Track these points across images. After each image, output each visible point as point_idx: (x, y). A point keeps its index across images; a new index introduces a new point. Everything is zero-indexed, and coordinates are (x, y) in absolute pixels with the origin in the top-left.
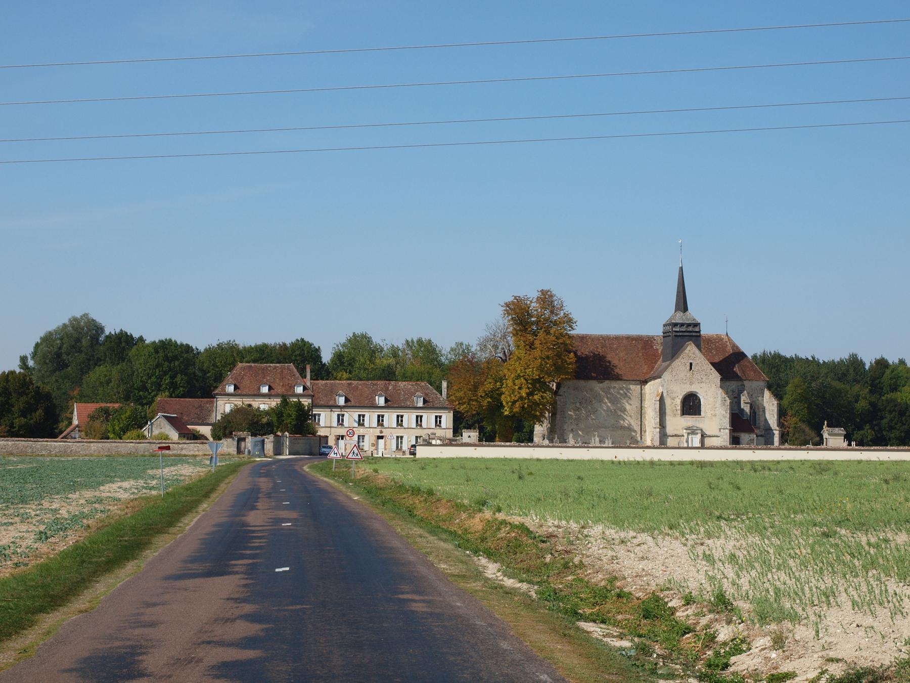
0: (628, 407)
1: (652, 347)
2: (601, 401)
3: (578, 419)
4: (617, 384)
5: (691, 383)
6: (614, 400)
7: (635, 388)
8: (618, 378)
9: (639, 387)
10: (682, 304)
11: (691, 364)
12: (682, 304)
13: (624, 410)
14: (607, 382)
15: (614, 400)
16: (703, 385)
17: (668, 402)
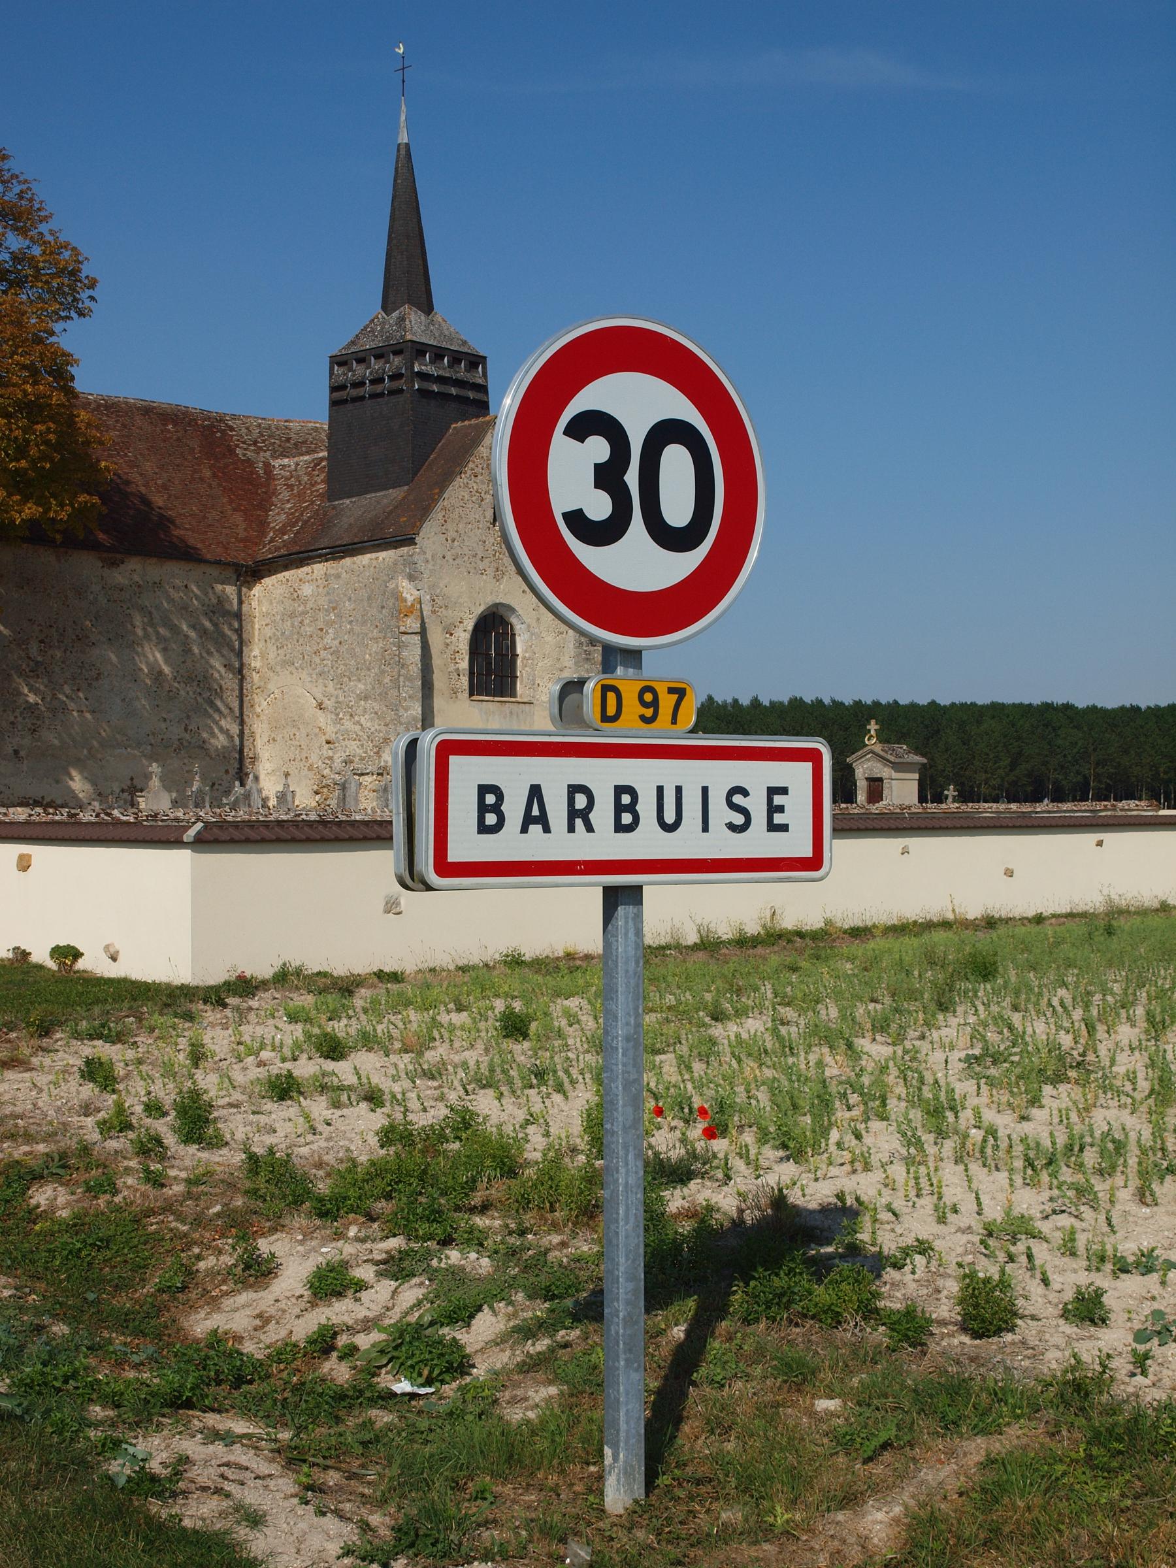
1: (231, 451)
17: (436, 638)
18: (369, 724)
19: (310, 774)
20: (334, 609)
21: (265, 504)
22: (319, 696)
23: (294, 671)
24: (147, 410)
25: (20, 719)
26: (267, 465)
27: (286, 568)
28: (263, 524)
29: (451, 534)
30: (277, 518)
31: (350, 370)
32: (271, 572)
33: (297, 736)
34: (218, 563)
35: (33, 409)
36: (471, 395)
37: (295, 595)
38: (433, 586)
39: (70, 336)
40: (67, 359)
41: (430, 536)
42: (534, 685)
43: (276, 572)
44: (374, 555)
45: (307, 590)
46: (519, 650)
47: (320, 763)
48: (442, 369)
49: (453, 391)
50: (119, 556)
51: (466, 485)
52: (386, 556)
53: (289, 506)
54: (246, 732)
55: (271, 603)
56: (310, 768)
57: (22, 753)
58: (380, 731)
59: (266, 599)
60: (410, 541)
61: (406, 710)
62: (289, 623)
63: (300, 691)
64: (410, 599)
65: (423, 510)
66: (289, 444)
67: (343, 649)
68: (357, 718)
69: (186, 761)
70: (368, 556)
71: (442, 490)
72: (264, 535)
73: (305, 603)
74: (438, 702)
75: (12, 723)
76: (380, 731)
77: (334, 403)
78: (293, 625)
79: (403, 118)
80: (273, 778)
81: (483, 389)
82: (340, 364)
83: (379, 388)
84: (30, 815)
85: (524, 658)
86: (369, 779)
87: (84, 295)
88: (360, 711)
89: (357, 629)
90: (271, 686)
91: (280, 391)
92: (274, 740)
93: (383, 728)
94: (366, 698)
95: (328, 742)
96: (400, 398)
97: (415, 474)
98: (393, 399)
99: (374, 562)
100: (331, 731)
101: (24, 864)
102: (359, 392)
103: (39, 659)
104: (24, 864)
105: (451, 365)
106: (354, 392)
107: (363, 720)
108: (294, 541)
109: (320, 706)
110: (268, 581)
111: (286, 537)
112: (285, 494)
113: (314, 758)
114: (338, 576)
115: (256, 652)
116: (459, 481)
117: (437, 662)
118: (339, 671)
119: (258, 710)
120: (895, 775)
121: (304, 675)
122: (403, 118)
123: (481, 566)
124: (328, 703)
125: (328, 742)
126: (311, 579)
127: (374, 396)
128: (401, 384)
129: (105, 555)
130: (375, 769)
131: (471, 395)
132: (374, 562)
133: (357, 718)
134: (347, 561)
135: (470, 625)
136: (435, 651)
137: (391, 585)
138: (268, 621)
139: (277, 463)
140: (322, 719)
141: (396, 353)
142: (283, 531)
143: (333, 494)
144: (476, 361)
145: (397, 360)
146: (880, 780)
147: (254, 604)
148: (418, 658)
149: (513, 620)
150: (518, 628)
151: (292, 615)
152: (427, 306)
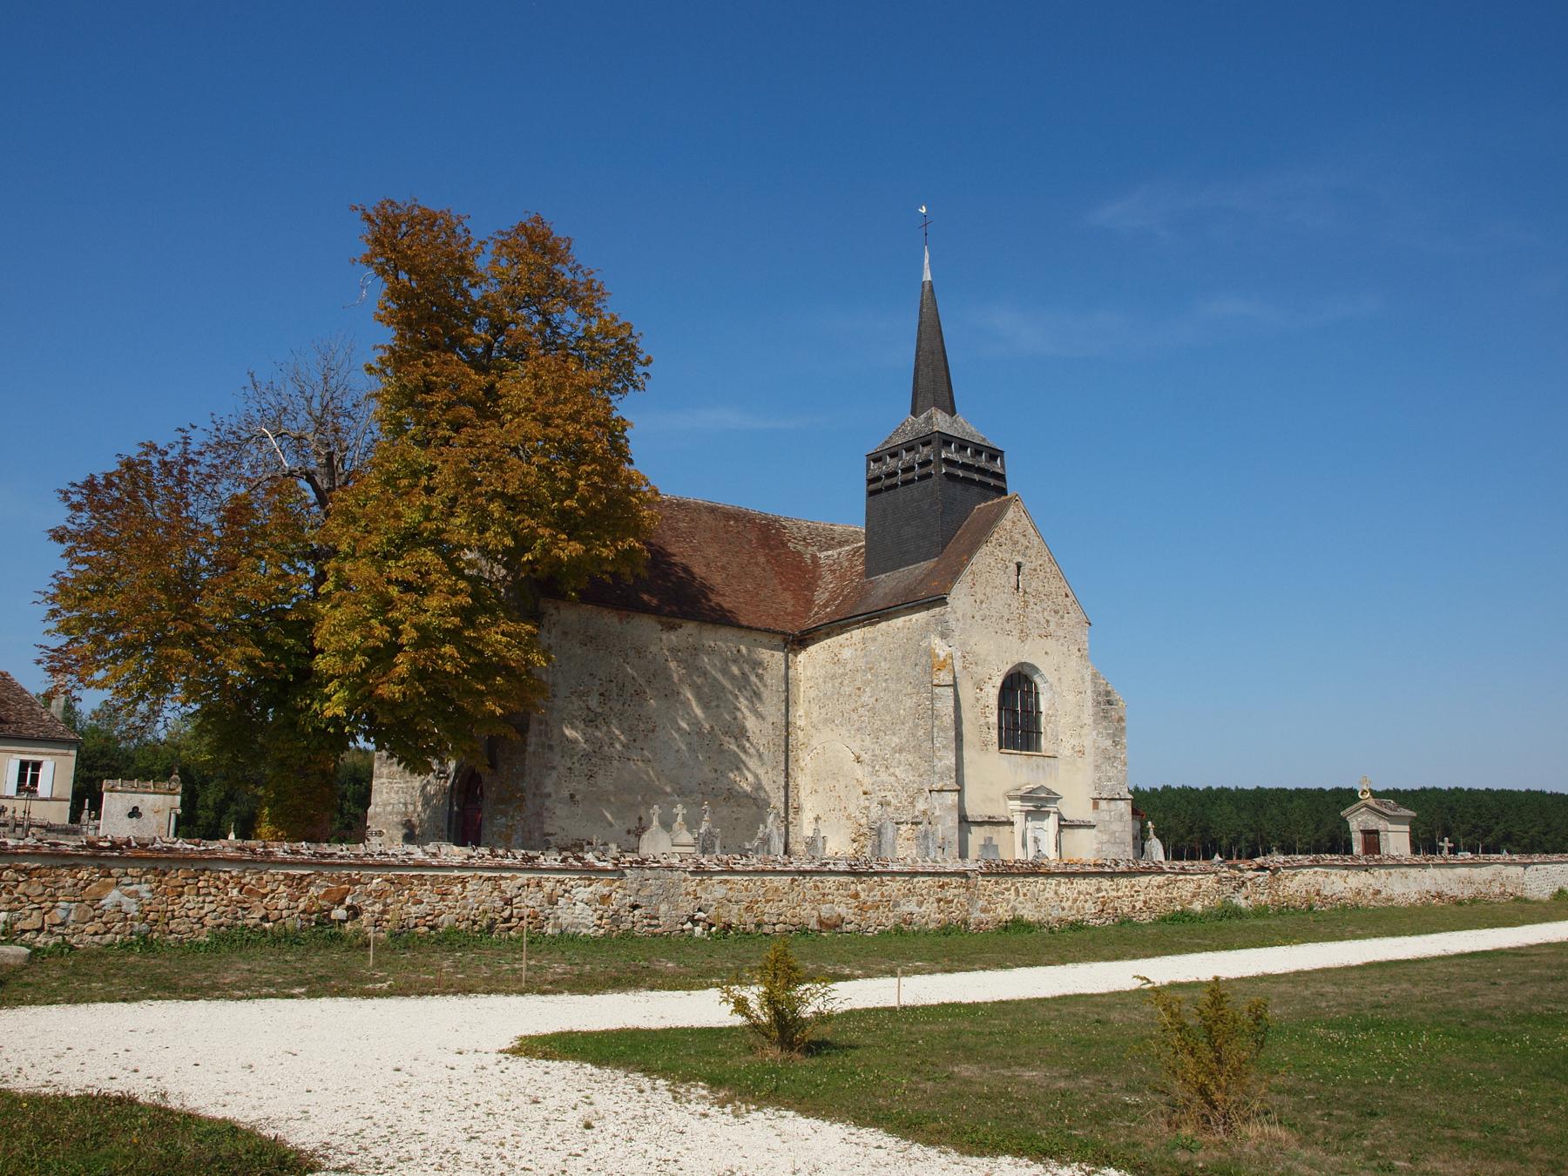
0: (751, 723)
1: (784, 545)
2: (670, 695)
3: (596, 756)
4: (719, 641)
5: (1024, 636)
6: (713, 698)
7: (773, 658)
8: (723, 619)
9: (779, 655)
10: (933, 382)
11: (1019, 566)
12: (933, 382)
13: (740, 733)
14: (690, 627)
15: (713, 698)
16: (1049, 644)
19: (849, 823)
21: (811, 586)
22: (858, 751)
24: (713, 510)
26: (814, 557)
27: (828, 635)
28: (810, 602)
29: (980, 596)
30: (821, 596)
32: (814, 641)
34: (767, 631)
35: (575, 453)
36: (992, 482)
38: (963, 644)
39: (625, 407)
40: (623, 424)
41: (959, 597)
42: (1057, 740)
43: (819, 640)
45: (846, 654)
46: (1042, 708)
48: (967, 457)
49: (977, 477)
51: (992, 553)
52: (920, 617)
56: (848, 818)
57: (578, 797)
59: (812, 662)
60: (942, 601)
64: (942, 655)
65: (954, 574)
66: (831, 542)
67: (879, 705)
72: (810, 610)
73: (844, 666)
74: (968, 754)
77: (871, 493)
81: (1001, 477)
82: (875, 461)
83: (910, 475)
84: (470, 857)
87: (639, 369)
88: (895, 763)
89: (892, 686)
90: (814, 742)
91: (829, 506)
94: (901, 751)
97: (944, 547)
98: (924, 483)
102: (893, 480)
105: (973, 456)
106: (888, 482)
107: (897, 772)
108: (832, 613)
109: (858, 760)
110: (811, 649)
112: (829, 577)
113: (852, 809)
114: (875, 639)
115: (801, 712)
116: (985, 549)
117: (966, 715)
119: (802, 764)
120: (1391, 827)
121: (843, 731)
123: (1007, 627)
124: (865, 757)
126: (849, 645)
127: (905, 483)
128: (931, 469)
129: (664, 619)
130: (910, 819)
131: (992, 482)
134: (883, 625)
135: (998, 682)
136: (965, 705)
137: (924, 644)
139: (822, 555)
140: (860, 772)
141: (924, 445)
142: (826, 606)
143: (868, 573)
144: (994, 454)
145: (926, 450)
146: (1377, 832)
147: (800, 669)
148: (951, 710)
149: (1037, 679)
150: (1042, 686)
151: (833, 677)
152: (952, 411)
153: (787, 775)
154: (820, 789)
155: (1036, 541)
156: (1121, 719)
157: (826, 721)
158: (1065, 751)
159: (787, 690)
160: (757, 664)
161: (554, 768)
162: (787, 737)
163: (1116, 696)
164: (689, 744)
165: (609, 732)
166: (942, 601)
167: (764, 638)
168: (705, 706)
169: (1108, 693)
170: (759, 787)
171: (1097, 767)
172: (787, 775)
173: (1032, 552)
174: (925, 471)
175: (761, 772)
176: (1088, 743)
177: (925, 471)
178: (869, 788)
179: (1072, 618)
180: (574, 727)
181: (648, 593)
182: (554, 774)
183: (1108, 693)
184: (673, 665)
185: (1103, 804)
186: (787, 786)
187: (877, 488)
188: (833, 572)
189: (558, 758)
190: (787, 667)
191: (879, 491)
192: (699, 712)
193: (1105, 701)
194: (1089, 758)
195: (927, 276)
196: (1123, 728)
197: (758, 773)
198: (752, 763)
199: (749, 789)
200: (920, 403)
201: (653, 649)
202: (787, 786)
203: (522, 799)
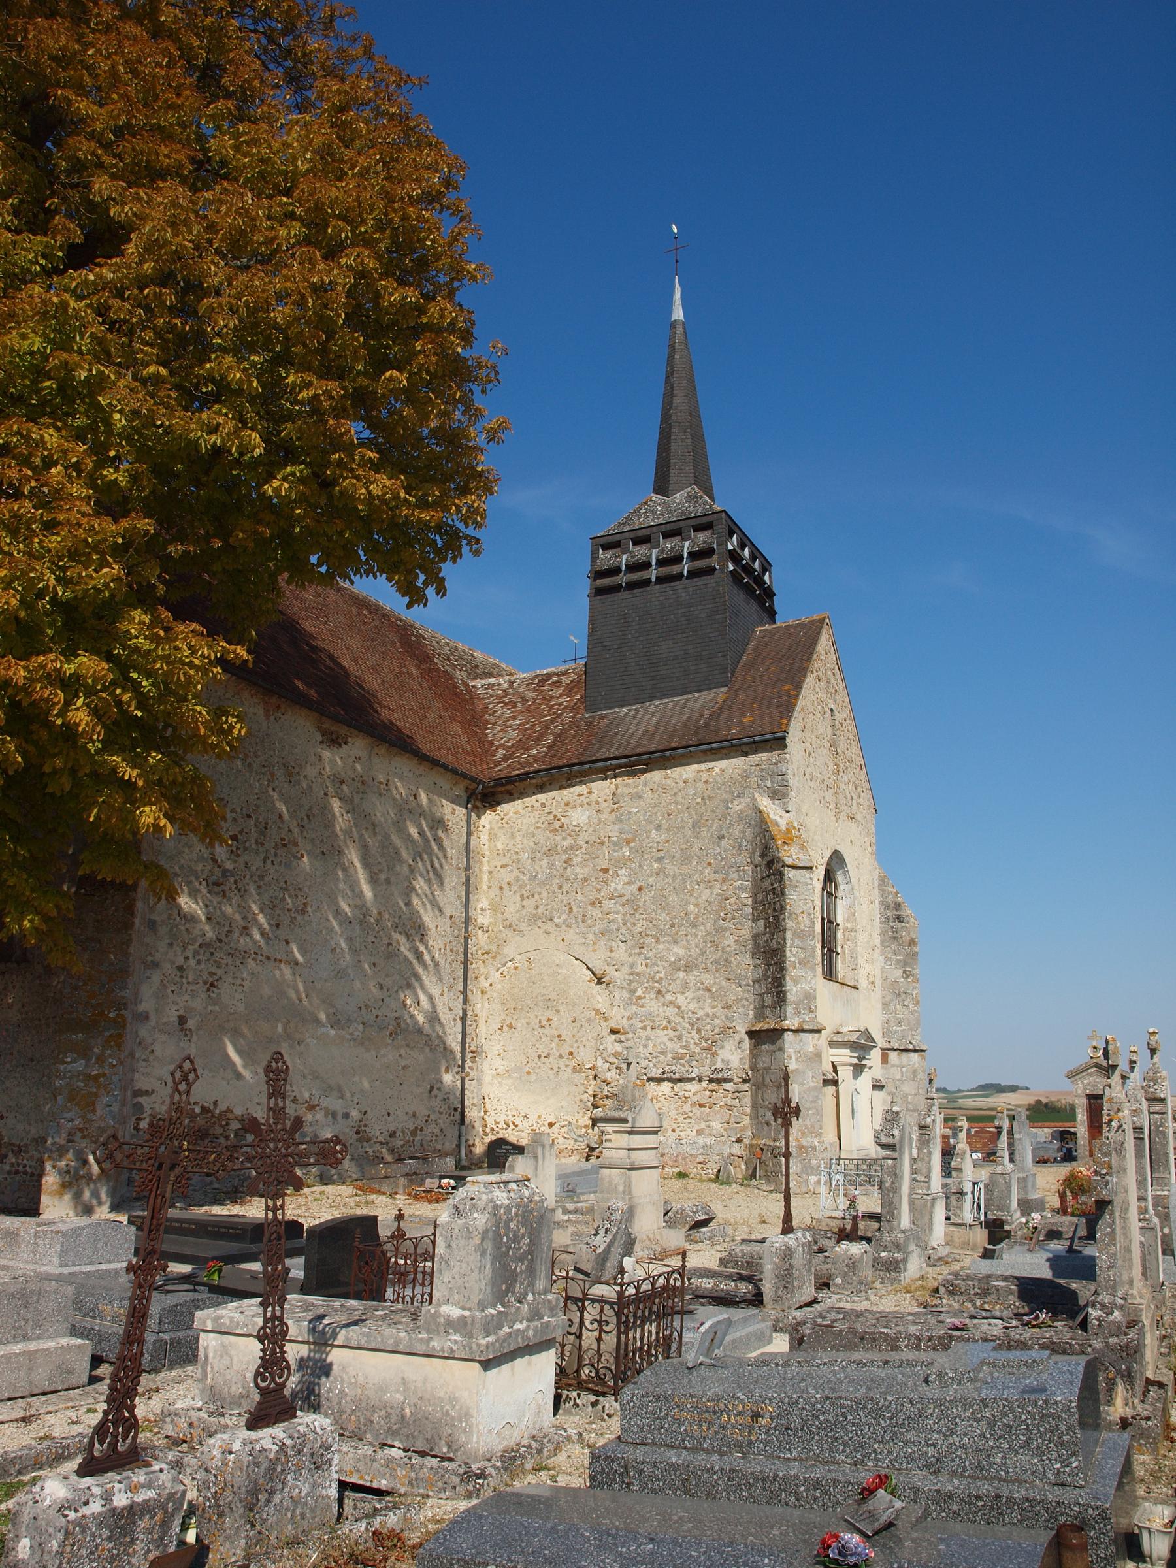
0: (428, 918)
2: (330, 853)
3: (222, 948)
4: (400, 779)
7: (454, 814)
8: (396, 741)
9: (461, 812)
13: (417, 931)
14: (358, 746)
15: (384, 867)
18: (692, 1006)
19: (578, 1078)
20: (628, 842)
22: (599, 967)
23: (552, 929)
25: (192, 962)
27: (541, 788)
31: (626, 551)
32: (511, 797)
33: (555, 1022)
37: (557, 824)
43: (522, 795)
44: (703, 766)
47: (600, 1062)
50: (343, 730)
53: (517, 722)
54: (469, 1013)
55: (513, 836)
57: (191, 1023)
58: (715, 1016)
61: (796, 982)
62: (545, 863)
63: (562, 957)
67: (646, 896)
68: (669, 997)
69: (403, 1052)
70: (695, 767)
71: (798, 687)
73: (575, 834)
75: (180, 968)
76: (715, 1016)
77: (599, 592)
78: (551, 865)
79: (677, 295)
80: (507, 1082)
82: (606, 547)
85: (845, 929)
86: (692, 1087)
89: (672, 868)
90: (509, 951)
92: (510, 1026)
93: (721, 1012)
94: (688, 968)
95: (614, 1032)
96: (710, 580)
99: (705, 776)
100: (618, 1017)
101: (529, 1363)
103: (229, 865)
104: (529, 1363)
106: (635, 576)
107: (681, 1000)
110: (507, 808)
111: (533, 752)
113: (586, 1055)
115: (484, 903)
118: (638, 928)
121: (571, 935)
122: (677, 295)
124: (612, 973)
125: (614, 1032)
126: (585, 805)
128: (714, 561)
130: (707, 1072)
132: (705, 776)
133: (669, 997)
134: (656, 776)
137: (736, 806)
138: (506, 861)
139: (478, 683)
141: (697, 529)
142: (523, 745)
143: (589, 703)
145: (701, 536)
147: (484, 838)
150: (842, 887)
151: (551, 852)
153: (465, 1001)
154: (520, 1024)
155: (841, 686)
156: (912, 942)
157: (534, 919)
158: (863, 983)
159: (468, 868)
160: (438, 824)
161: (156, 965)
162: (466, 939)
163: (907, 911)
164: (350, 940)
165: (243, 909)
166: (778, 743)
167: (444, 781)
168: (373, 880)
169: (898, 906)
170: (433, 1018)
171: (885, 1005)
172: (465, 1001)
173: (839, 699)
174: (702, 563)
175: (435, 991)
176: (878, 972)
177: (702, 563)
178: (623, 1024)
179: (866, 799)
180: (193, 894)
181: (300, 679)
182: (156, 978)
183: (898, 906)
184: (336, 804)
185: (893, 1055)
186: (464, 1019)
187: (604, 584)
188: (513, 704)
189: (162, 946)
190: (469, 834)
191: (616, 588)
192: (368, 892)
193: (894, 916)
194: (878, 993)
195: (678, 314)
196: (915, 954)
197: (432, 998)
198: (428, 980)
199: (421, 1019)
200: (673, 475)
201: (311, 771)
202: (464, 1019)
203: (120, 1023)
